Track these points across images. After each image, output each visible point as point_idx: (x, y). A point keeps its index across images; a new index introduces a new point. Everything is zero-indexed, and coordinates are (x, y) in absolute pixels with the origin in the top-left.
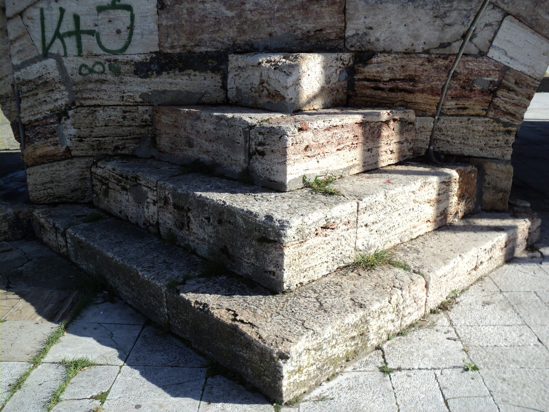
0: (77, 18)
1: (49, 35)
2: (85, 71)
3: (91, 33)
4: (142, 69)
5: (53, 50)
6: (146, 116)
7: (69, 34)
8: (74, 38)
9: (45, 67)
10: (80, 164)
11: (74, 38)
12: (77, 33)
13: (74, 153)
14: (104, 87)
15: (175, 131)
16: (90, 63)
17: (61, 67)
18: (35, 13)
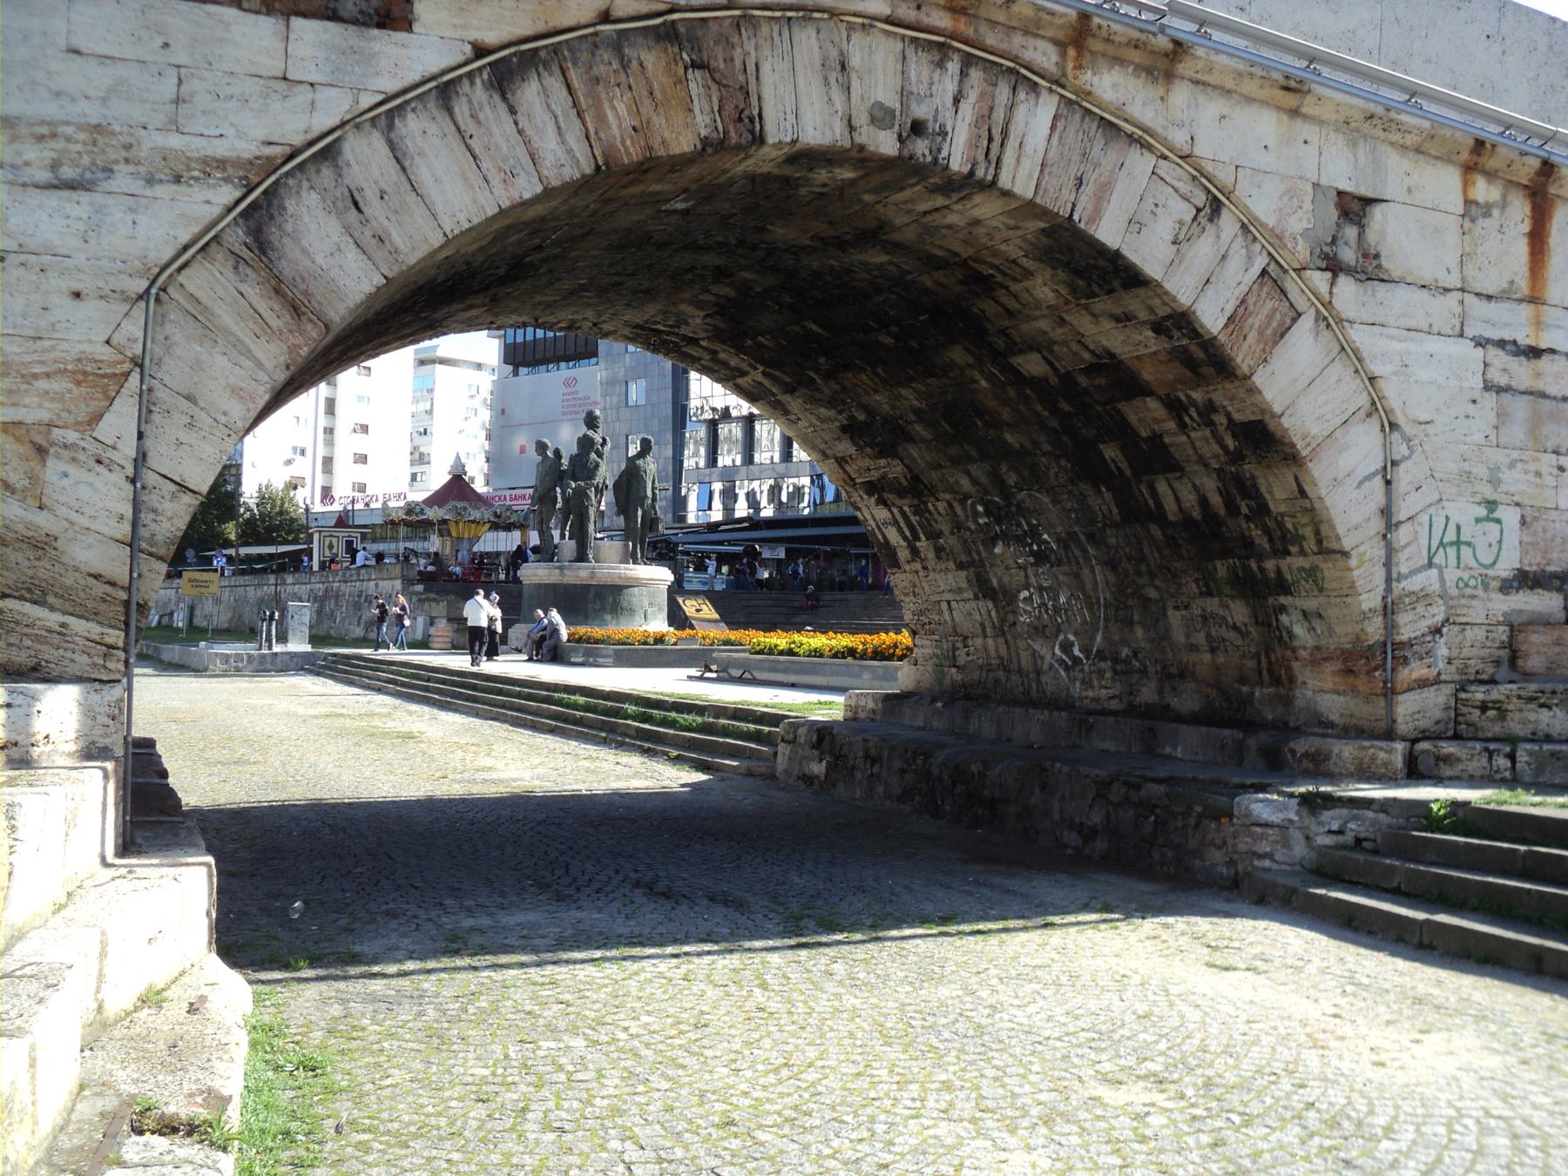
0: (1458, 528)
1: (1435, 544)
2: (1461, 585)
3: (1469, 544)
4: (1506, 587)
5: (1436, 560)
6: (1504, 638)
7: (1452, 544)
8: (1454, 548)
9: (1428, 578)
10: (1448, 689)
11: (1454, 548)
12: (1457, 543)
13: (1443, 677)
14: (1474, 603)
15: (1557, 649)
16: (1466, 577)
17: (1442, 580)
18: (1424, 518)
